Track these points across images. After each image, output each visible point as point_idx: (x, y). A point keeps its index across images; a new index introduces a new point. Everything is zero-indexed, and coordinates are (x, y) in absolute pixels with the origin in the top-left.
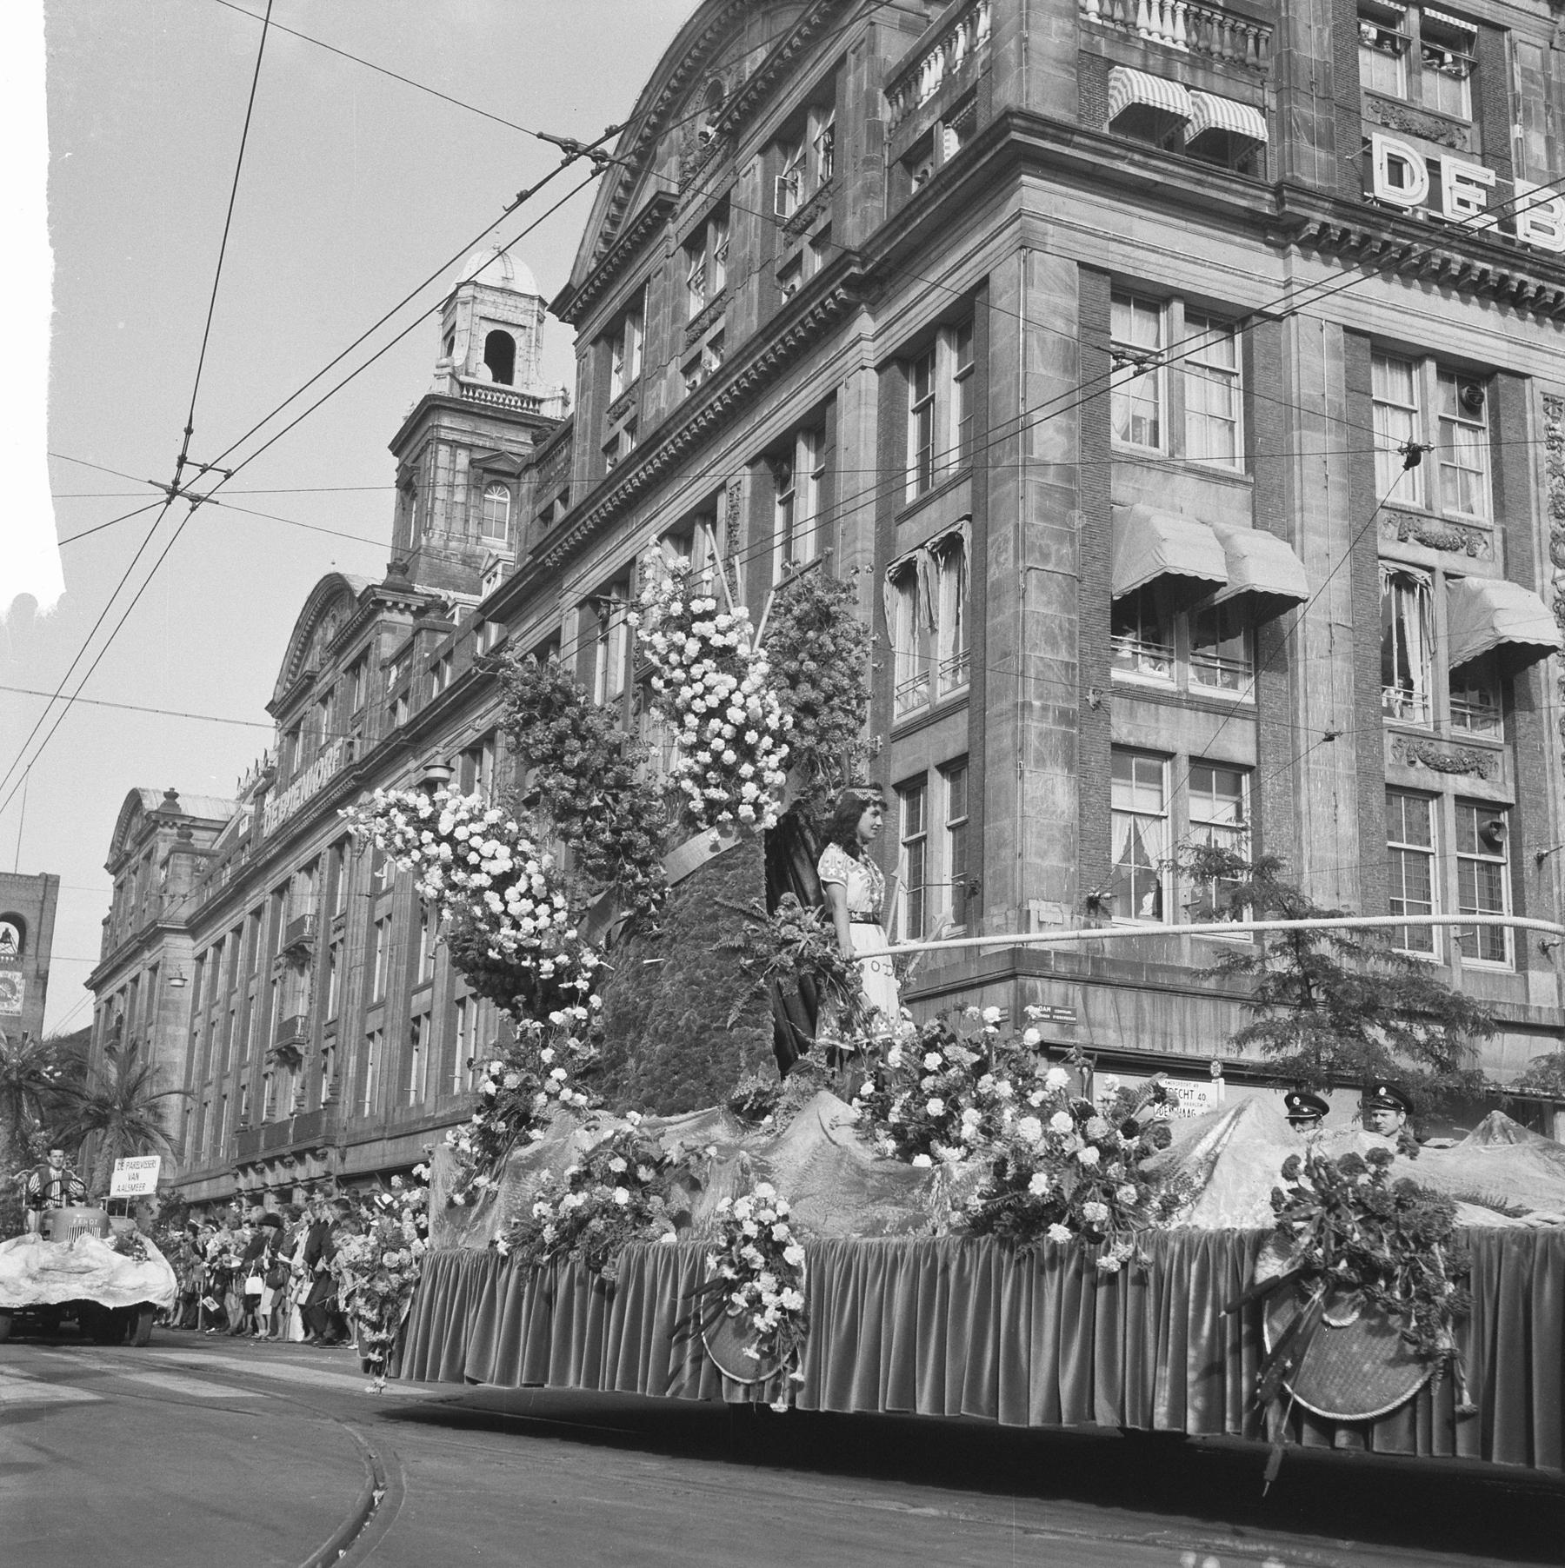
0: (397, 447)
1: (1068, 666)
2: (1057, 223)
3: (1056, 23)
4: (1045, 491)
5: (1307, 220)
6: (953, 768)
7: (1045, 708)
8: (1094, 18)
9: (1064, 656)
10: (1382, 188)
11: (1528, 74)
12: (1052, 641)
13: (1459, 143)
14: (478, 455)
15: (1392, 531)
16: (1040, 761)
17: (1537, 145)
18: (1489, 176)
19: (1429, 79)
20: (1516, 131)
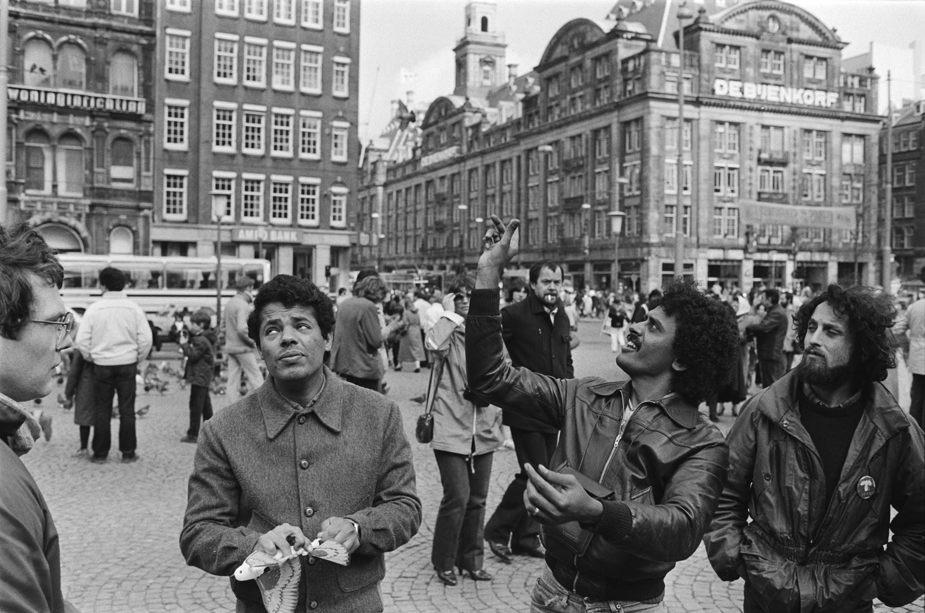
0: (455, 50)
6: (636, 207)
14: (482, 57)
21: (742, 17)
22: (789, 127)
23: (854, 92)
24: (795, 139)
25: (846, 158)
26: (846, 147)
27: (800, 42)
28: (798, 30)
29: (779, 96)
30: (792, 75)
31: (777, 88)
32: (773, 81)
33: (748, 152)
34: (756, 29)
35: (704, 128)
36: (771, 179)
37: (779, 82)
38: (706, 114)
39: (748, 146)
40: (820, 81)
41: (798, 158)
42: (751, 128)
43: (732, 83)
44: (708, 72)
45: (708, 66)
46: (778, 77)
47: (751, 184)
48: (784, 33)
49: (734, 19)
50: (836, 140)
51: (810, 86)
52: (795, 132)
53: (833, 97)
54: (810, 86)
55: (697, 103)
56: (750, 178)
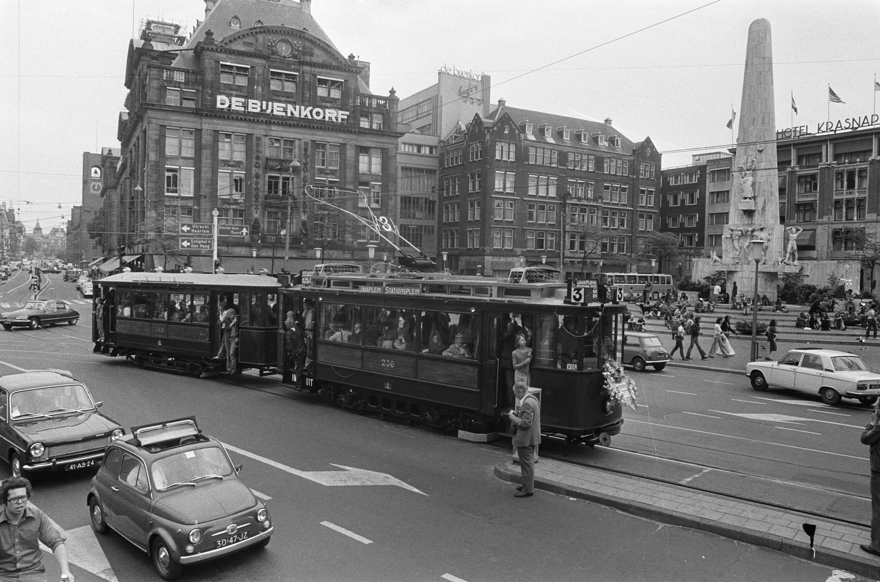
1: (156, 194)
2: (154, 118)
3: (155, 82)
4: (152, 166)
5: (202, 114)
7: (151, 201)
8: (165, 79)
9: (155, 193)
10: (219, 106)
11: (259, 75)
12: (153, 191)
13: (243, 91)
15: (223, 165)
16: (150, 210)
17: (260, 89)
18: (243, 100)
19: (238, 77)
20: (256, 87)
21: (250, 39)
22: (299, 139)
23: (372, 111)
24: (306, 150)
25: (363, 167)
26: (363, 159)
27: (312, 65)
28: (311, 55)
29: (286, 112)
30: (303, 94)
31: (284, 105)
32: (283, 99)
33: (254, 161)
34: (266, 52)
35: (206, 138)
36: (267, 183)
37: (291, 100)
38: (208, 125)
39: (254, 156)
40: (335, 100)
41: (308, 166)
42: (258, 139)
43: (234, 99)
44: (212, 88)
45: (212, 82)
46: (288, 95)
47: (257, 189)
48: (294, 57)
49: (241, 41)
50: (350, 153)
51: (324, 104)
52: (306, 143)
53: (342, 115)
54: (324, 104)
55: (197, 113)
56: (257, 183)
